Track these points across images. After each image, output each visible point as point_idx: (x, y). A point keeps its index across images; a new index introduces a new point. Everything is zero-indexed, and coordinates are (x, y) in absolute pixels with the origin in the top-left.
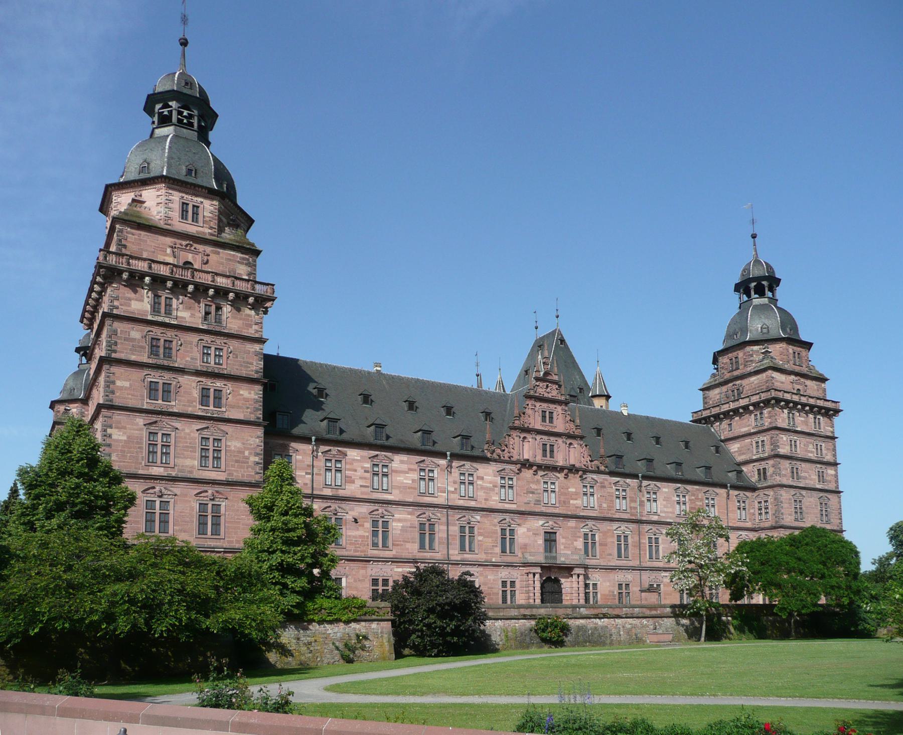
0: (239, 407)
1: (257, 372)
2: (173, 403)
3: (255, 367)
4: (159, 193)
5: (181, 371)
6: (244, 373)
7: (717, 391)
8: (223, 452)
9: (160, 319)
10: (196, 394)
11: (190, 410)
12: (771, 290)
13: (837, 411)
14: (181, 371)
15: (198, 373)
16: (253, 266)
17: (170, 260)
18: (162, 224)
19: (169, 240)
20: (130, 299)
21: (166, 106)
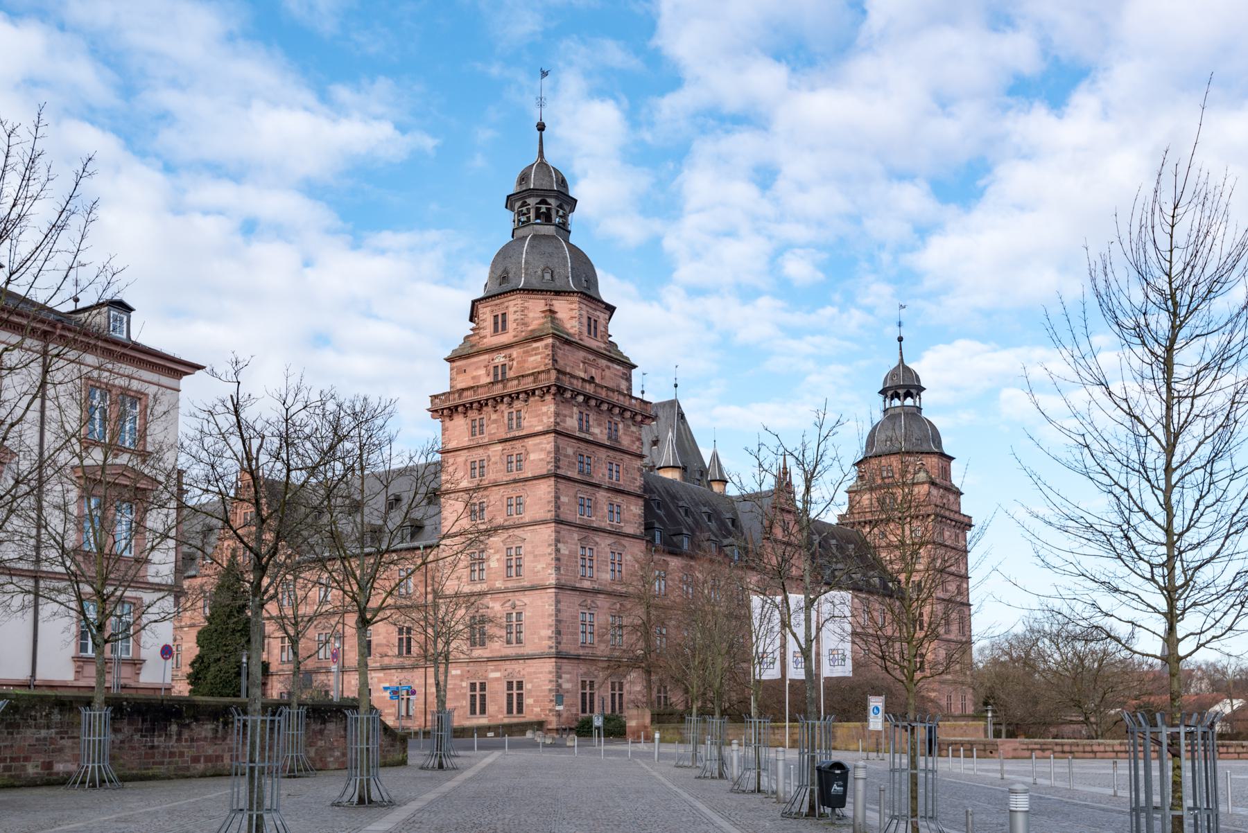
0: (631, 522)
1: (640, 488)
2: (594, 518)
3: (637, 484)
4: (573, 306)
5: (598, 486)
6: (631, 489)
7: (867, 496)
8: (595, 562)
9: (583, 435)
10: (606, 509)
11: (603, 525)
12: (918, 394)
13: (971, 526)
14: (598, 486)
15: (609, 489)
16: (629, 379)
17: (582, 375)
18: (576, 339)
19: (582, 354)
20: (565, 416)
21: (544, 202)
